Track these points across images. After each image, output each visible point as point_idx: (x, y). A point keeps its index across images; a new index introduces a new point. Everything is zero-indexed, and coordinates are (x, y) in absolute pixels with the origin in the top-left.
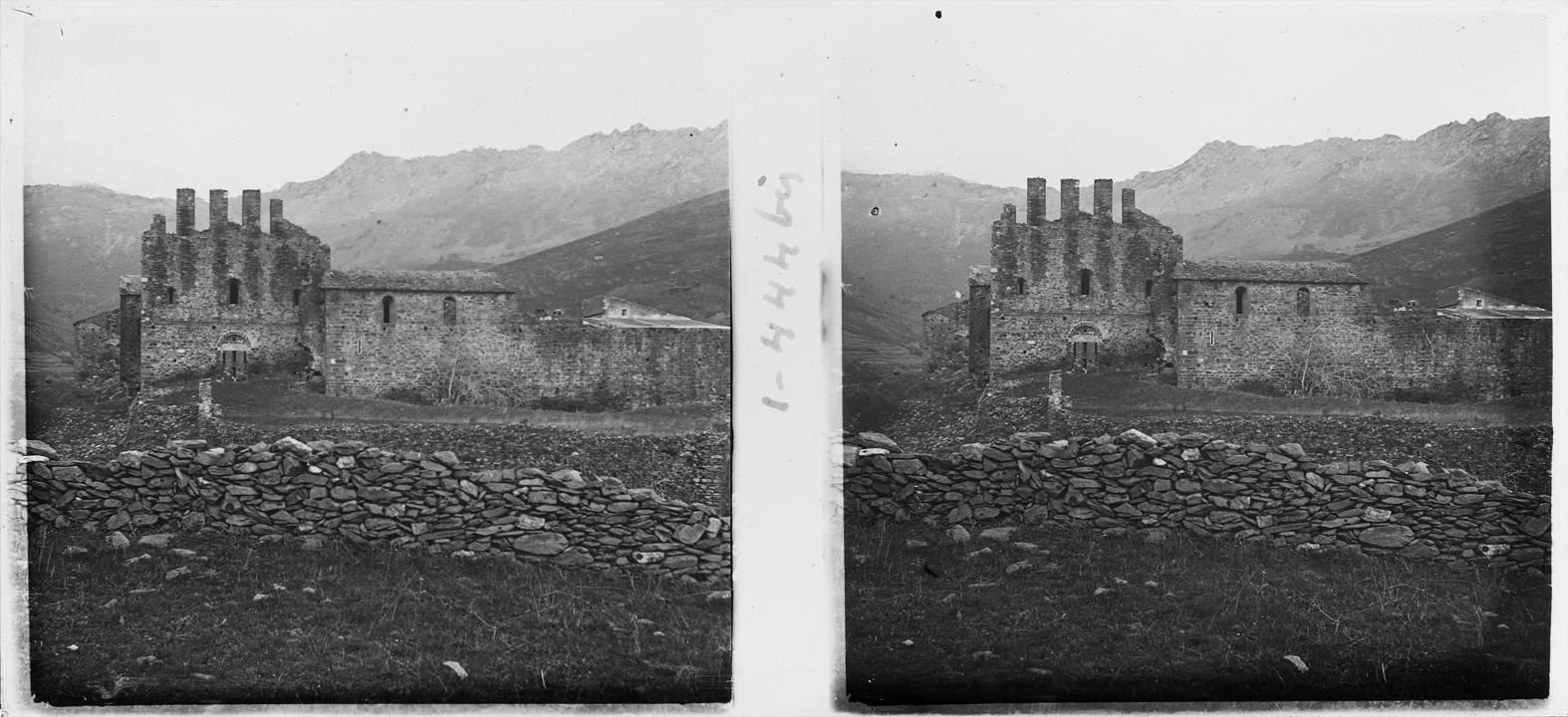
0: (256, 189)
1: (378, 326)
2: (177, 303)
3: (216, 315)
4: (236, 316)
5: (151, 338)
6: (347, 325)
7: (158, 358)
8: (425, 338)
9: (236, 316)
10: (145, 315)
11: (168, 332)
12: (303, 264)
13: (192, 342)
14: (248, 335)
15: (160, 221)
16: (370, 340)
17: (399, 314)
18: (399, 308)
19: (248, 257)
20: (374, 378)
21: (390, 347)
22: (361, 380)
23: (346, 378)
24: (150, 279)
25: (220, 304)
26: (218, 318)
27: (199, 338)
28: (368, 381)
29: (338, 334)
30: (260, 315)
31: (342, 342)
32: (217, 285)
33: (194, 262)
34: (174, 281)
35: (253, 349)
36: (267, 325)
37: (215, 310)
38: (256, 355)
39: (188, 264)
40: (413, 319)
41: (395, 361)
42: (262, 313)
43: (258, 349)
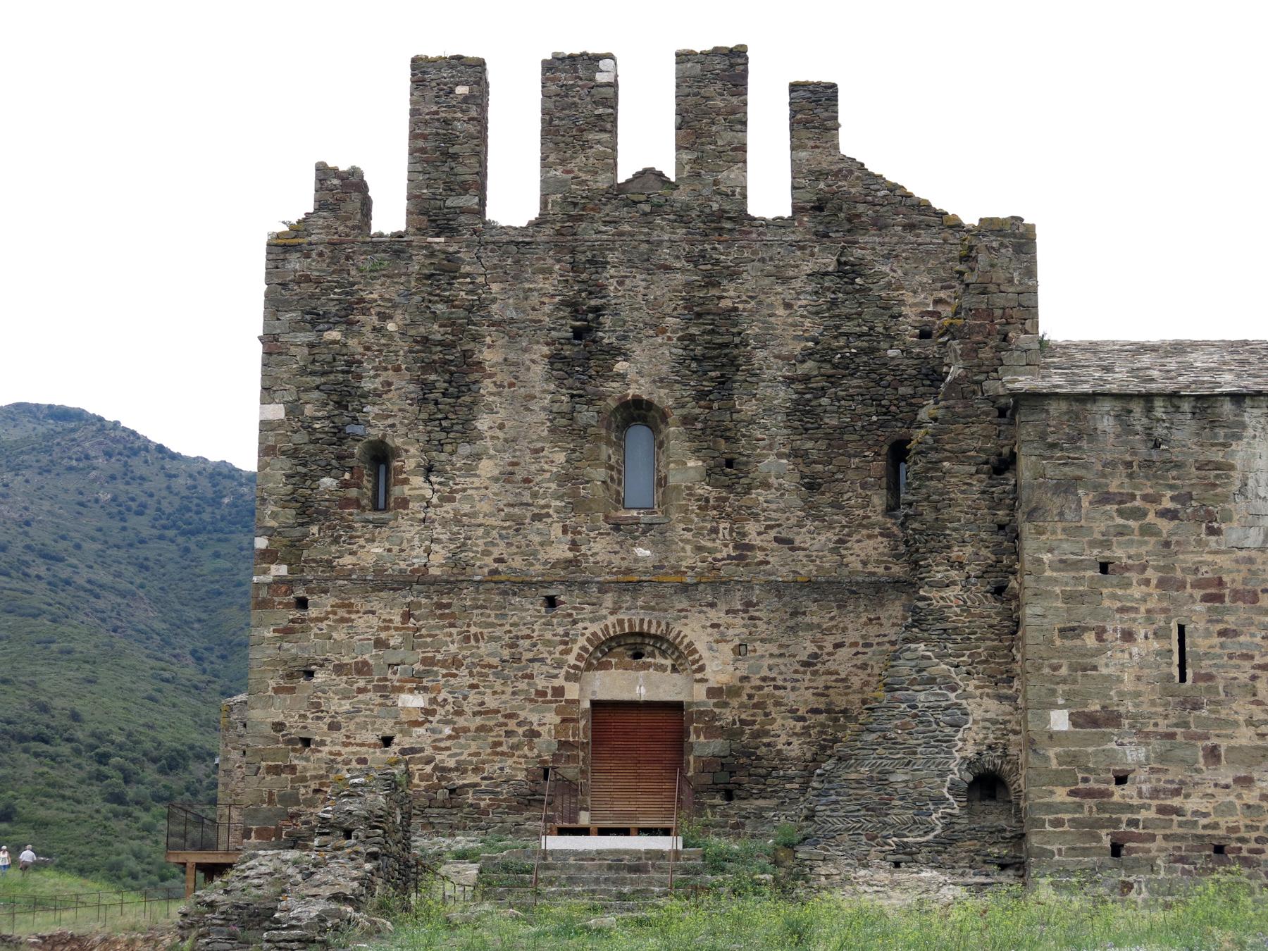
0: (731, 44)
2: (404, 503)
3: (561, 551)
4: (641, 552)
5: (291, 648)
6: (1119, 553)
7: (317, 730)
9: (641, 552)
10: (269, 556)
11: (360, 622)
12: (925, 335)
13: (457, 663)
14: (694, 630)
15: (342, 191)
16: (1231, 621)
19: (696, 311)
22: (1192, 804)
23: (1118, 794)
24: (293, 410)
25: (577, 505)
26: (569, 563)
27: (484, 648)
28: (1228, 809)
30: (743, 548)
31: (1100, 633)
32: (566, 428)
33: (476, 338)
34: (390, 415)
35: (712, 692)
36: (777, 589)
37: (557, 530)
38: (728, 716)
39: (447, 346)
42: (757, 541)
43: (733, 691)
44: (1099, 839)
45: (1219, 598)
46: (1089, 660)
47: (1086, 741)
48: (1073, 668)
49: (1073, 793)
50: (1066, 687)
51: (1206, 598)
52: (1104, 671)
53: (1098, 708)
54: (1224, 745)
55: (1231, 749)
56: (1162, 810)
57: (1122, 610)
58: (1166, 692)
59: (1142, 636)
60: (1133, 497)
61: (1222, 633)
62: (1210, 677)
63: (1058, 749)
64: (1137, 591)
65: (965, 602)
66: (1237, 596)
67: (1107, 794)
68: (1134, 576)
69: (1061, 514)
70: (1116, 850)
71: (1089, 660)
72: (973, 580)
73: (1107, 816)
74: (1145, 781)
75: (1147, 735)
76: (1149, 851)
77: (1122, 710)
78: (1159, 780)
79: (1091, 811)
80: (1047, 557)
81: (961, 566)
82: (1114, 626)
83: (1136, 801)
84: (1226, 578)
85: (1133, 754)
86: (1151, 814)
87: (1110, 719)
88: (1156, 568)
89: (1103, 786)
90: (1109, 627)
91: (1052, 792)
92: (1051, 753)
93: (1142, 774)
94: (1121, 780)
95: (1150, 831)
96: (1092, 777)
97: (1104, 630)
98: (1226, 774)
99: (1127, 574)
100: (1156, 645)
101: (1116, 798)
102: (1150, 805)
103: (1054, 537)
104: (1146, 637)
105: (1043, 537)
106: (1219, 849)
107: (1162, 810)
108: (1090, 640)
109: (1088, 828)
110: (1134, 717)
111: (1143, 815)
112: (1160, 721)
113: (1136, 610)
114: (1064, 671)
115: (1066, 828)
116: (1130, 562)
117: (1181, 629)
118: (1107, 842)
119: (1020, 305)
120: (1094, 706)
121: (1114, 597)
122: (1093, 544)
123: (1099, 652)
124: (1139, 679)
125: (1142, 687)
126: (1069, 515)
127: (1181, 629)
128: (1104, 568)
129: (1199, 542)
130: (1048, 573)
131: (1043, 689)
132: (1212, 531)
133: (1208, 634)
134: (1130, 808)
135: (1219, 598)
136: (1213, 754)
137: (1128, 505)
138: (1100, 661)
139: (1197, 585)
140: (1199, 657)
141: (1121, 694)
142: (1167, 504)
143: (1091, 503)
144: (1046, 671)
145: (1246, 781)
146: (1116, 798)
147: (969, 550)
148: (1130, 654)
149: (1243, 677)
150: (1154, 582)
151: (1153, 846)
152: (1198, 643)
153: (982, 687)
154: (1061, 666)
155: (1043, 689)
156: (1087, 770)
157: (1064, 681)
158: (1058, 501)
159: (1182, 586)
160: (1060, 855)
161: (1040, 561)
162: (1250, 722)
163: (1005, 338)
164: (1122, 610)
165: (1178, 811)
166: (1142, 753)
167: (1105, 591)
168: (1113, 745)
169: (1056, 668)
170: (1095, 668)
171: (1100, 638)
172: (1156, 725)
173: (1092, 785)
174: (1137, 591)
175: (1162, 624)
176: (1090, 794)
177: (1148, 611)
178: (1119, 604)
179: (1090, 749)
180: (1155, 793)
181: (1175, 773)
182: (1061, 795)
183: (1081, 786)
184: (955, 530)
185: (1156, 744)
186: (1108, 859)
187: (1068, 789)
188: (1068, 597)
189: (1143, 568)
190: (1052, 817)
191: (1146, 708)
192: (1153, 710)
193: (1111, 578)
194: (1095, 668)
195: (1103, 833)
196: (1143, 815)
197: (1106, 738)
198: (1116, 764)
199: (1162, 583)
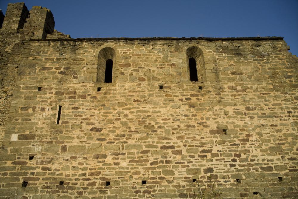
1: (91, 87)
6: (45, 85)
8: (161, 100)
16: (76, 105)
17: (123, 69)
18: (123, 62)
20: (75, 164)
21: (106, 114)
22: (53, 167)
23: (29, 163)
28: (67, 168)
29: (30, 98)
31: (34, 109)
40: (141, 75)
41: (112, 136)
44: (19, 180)
45: (74, 98)
46: (28, 117)
47: (22, 145)
48: (23, 120)
49: (13, 163)
50: (19, 126)
51: (70, 98)
52: (33, 121)
53: (28, 133)
54: (68, 145)
55: (70, 147)
56: (43, 169)
57: (42, 101)
58: (52, 127)
59: (47, 109)
60: (52, 68)
61: (73, 108)
62: (67, 122)
63: (12, 147)
64: (48, 96)
65: (5, 103)
66: (80, 96)
67: (25, 163)
68: (48, 91)
69: (29, 74)
70: (25, 184)
71: (28, 117)
72: (9, 96)
73: (24, 171)
74: (39, 158)
75: (43, 142)
76: (36, 184)
77: (36, 133)
78: (44, 158)
79: (18, 170)
80: (22, 86)
81: (6, 92)
82: (38, 107)
83: (35, 166)
84: (77, 91)
85: (37, 148)
86: (39, 170)
87: (32, 137)
88: (55, 89)
89: (24, 160)
90: (37, 107)
91: (6, 163)
92: (9, 149)
93: (39, 156)
94: (31, 158)
95: (38, 177)
96: (21, 157)
97: (35, 108)
98: (67, 155)
99: (46, 91)
100: (51, 112)
101: (28, 165)
102: (39, 167)
103: (26, 80)
104: (49, 110)
105: (22, 80)
106: (62, 183)
107: (43, 169)
108: (30, 111)
109: (15, 176)
110: (40, 136)
111: (37, 170)
112: (48, 137)
113: (47, 101)
114: (19, 121)
115: (8, 176)
116: (48, 87)
117: (60, 107)
118: (21, 181)
119: (39, 26)
120: (27, 132)
121: (41, 97)
122: (37, 82)
123: (32, 115)
124: (44, 123)
125: (44, 126)
126: (32, 73)
127: (60, 107)
128: (39, 89)
129: (70, 81)
130: (22, 90)
131: (11, 127)
132: (75, 78)
133: (69, 108)
134: (35, 168)
135: (74, 98)
136: (64, 149)
137: (51, 70)
138: (33, 117)
139: (67, 93)
140: (64, 116)
141: (37, 129)
142: (62, 70)
143: (39, 70)
144: (14, 121)
145: (74, 158)
146: (28, 165)
147: (10, 88)
148: (42, 115)
149: (78, 122)
150: (54, 93)
151: (38, 182)
152: (64, 112)
153: (3, 129)
154: (19, 119)
155: (11, 127)
156: (21, 155)
157: (19, 124)
158: (29, 70)
159: (63, 94)
160: (3, 187)
161: (20, 87)
162: (78, 137)
163: (33, 34)
164: (42, 101)
165: (49, 169)
166: (40, 148)
167: (38, 96)
168: (31, 146)
169: (17, 120)
170: (30, 120)
171: (34, 110)
172: (46, 138)
173: (21, 160)
174: (48, 96)
175: (54, 106)
176: (19, 163)
177: (51, 102)
178: (42, 100)
179: (23, 147)
180: (42, 163)
181: (50, 155)
182: (9, 164)
183: (17, 160)
184: (7, 82)
185: (46, 145)
186: (20, 189)
187: (12, 161)
188: (26, 98)
189: (51, 89)
190: (3, 172)
191: (44, 133)
192: (47, 133)
193: (41, 92)
194: (30, 120)
195: (21, 177)
196: (37, 170)
197: (29, 143)
198: (31, 152)
199: (57, 93)
